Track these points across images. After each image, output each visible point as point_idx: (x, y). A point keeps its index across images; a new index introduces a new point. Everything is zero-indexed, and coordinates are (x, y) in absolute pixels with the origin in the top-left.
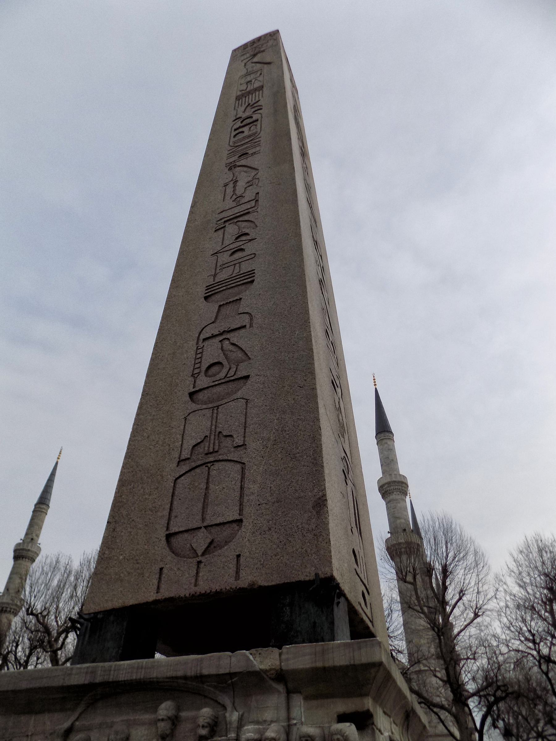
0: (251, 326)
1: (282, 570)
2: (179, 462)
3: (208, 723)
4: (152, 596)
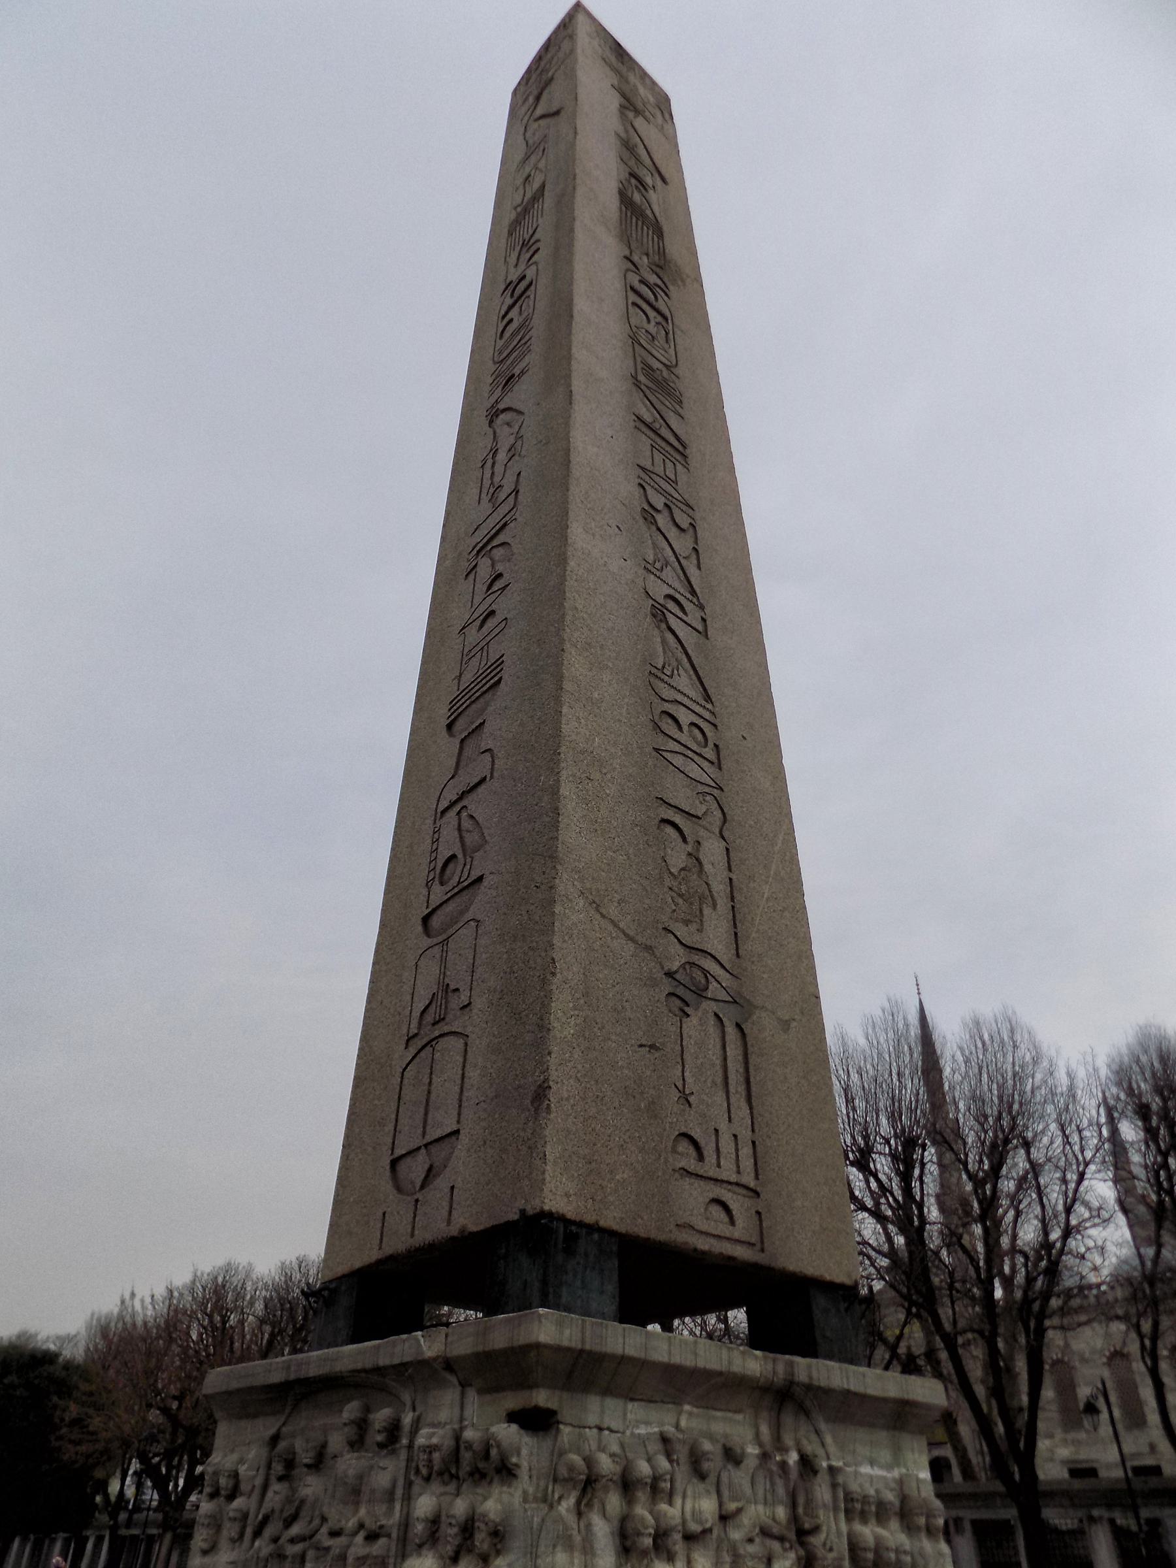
0: (492, 777)
2: (408, 1041)
3: (385, 1428)
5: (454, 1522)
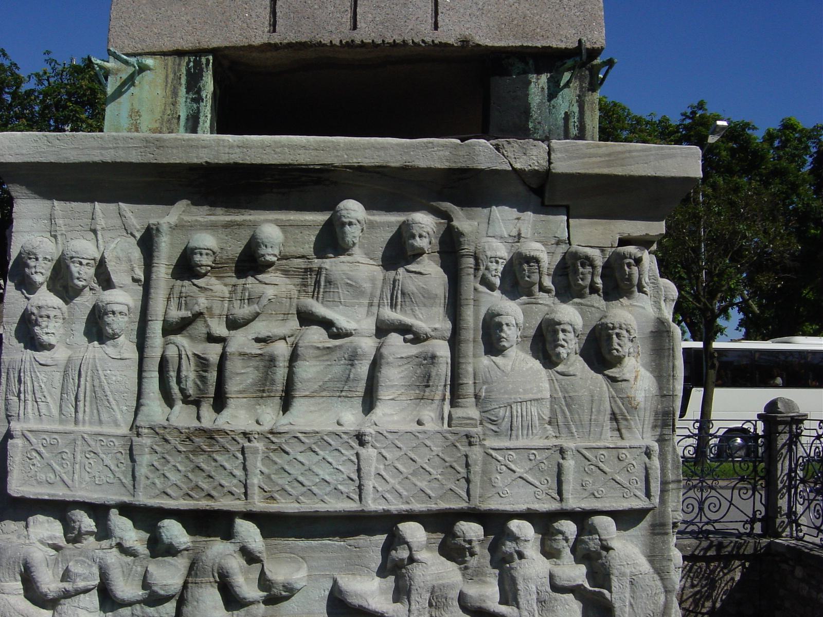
1: (517, 25)
4: (259, 36)
5: (569, 328)
